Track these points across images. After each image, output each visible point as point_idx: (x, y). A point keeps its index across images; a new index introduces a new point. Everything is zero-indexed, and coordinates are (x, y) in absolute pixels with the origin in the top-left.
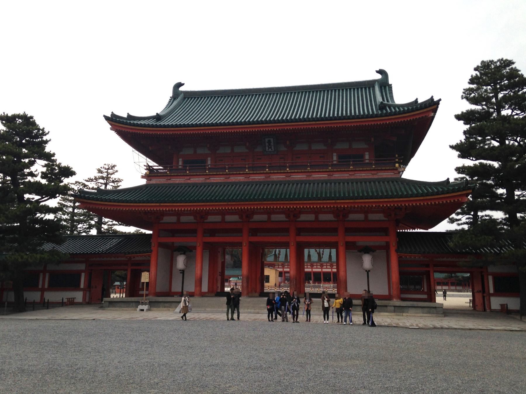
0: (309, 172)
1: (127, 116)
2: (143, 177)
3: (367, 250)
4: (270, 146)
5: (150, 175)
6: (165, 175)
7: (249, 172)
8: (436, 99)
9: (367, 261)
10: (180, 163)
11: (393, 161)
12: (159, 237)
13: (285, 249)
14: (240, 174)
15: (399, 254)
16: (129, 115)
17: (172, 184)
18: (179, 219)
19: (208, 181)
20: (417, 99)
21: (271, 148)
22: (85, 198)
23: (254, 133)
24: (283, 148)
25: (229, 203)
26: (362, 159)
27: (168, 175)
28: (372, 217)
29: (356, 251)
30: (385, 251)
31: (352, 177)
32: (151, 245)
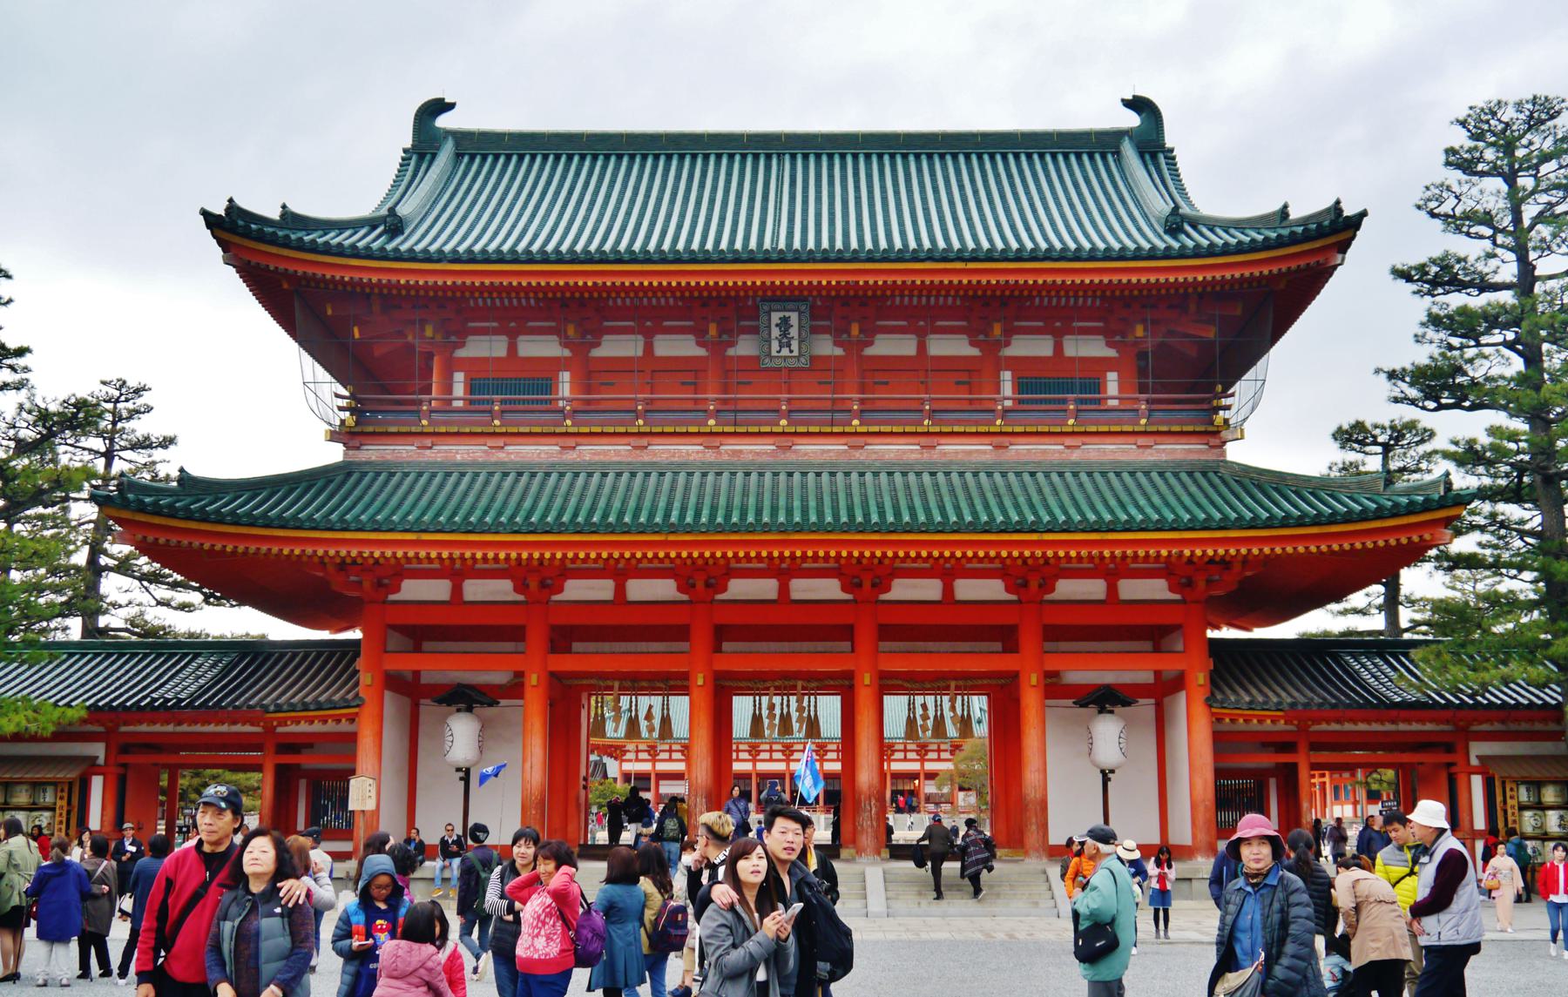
0: (928, 434)
1: (283, 216)
2: (334, 436)
3: (1105, 699)
4: (785, 340)
5: (356, 430)
6: (414, 429)
7: (720, 429)
8: (1349, 210)
9: (1108, 733)
10: (459, 390)
11: (1205, 406)
12: (386, 652)
13: (906, 697)
14: (687, 434)
15: (1214, 710)
16: (286, 213)
17: (441, 463)
18: (457, 591)
19: (571, 456)
21: (789, 345)
22: (142, 508)
23: (833, 293)
24: (826, 347)
25: (672, 538)
26: (1097, 396)
27: (425, 430)
28: (1131, 589)
29: (1069, 702)
30: (1152, 701)
31: (1075, 456)
32: (357, 684)
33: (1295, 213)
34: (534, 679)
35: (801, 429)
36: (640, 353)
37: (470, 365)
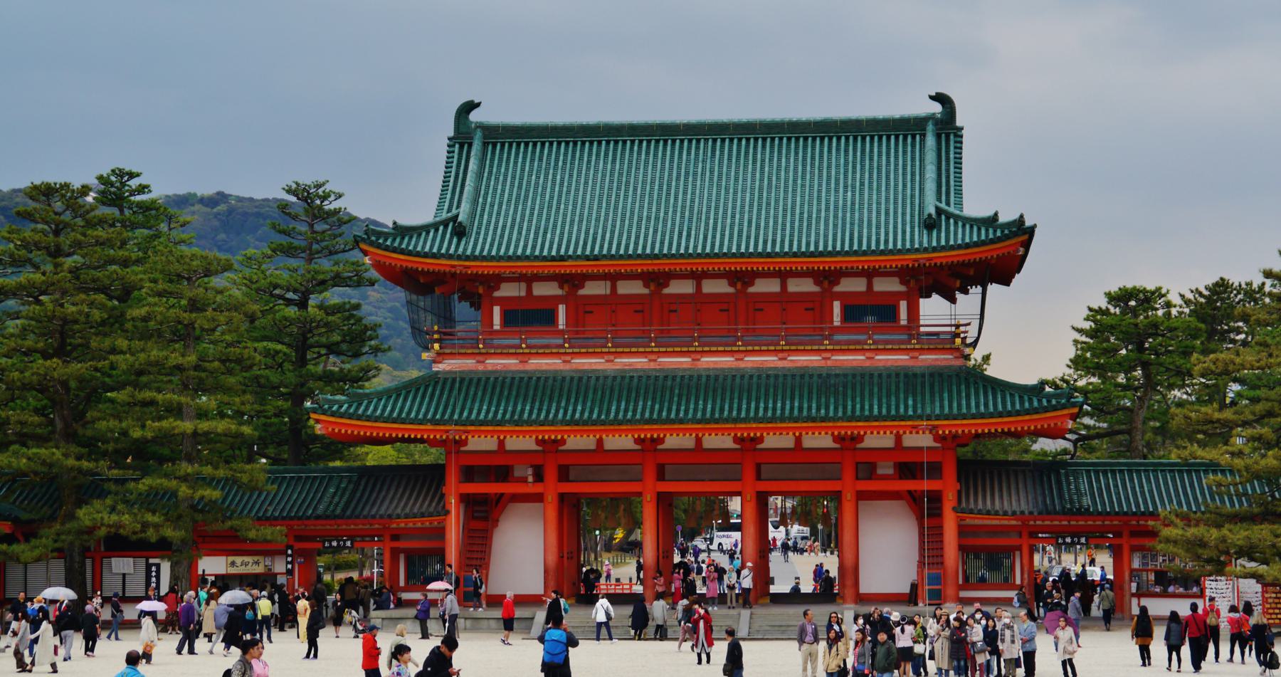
5: (442, 351)
20: (996, 214)
33: (1003, 219)
34: (550, 499)
35: (706, 349)
36: (608, 292)
37: (500, 301)
